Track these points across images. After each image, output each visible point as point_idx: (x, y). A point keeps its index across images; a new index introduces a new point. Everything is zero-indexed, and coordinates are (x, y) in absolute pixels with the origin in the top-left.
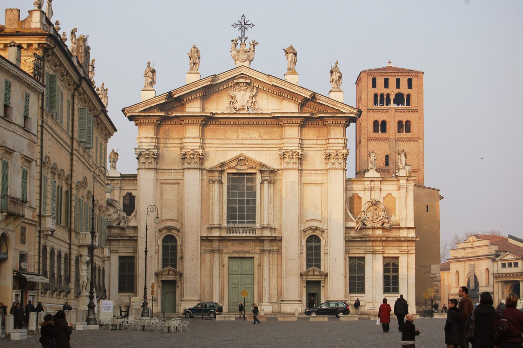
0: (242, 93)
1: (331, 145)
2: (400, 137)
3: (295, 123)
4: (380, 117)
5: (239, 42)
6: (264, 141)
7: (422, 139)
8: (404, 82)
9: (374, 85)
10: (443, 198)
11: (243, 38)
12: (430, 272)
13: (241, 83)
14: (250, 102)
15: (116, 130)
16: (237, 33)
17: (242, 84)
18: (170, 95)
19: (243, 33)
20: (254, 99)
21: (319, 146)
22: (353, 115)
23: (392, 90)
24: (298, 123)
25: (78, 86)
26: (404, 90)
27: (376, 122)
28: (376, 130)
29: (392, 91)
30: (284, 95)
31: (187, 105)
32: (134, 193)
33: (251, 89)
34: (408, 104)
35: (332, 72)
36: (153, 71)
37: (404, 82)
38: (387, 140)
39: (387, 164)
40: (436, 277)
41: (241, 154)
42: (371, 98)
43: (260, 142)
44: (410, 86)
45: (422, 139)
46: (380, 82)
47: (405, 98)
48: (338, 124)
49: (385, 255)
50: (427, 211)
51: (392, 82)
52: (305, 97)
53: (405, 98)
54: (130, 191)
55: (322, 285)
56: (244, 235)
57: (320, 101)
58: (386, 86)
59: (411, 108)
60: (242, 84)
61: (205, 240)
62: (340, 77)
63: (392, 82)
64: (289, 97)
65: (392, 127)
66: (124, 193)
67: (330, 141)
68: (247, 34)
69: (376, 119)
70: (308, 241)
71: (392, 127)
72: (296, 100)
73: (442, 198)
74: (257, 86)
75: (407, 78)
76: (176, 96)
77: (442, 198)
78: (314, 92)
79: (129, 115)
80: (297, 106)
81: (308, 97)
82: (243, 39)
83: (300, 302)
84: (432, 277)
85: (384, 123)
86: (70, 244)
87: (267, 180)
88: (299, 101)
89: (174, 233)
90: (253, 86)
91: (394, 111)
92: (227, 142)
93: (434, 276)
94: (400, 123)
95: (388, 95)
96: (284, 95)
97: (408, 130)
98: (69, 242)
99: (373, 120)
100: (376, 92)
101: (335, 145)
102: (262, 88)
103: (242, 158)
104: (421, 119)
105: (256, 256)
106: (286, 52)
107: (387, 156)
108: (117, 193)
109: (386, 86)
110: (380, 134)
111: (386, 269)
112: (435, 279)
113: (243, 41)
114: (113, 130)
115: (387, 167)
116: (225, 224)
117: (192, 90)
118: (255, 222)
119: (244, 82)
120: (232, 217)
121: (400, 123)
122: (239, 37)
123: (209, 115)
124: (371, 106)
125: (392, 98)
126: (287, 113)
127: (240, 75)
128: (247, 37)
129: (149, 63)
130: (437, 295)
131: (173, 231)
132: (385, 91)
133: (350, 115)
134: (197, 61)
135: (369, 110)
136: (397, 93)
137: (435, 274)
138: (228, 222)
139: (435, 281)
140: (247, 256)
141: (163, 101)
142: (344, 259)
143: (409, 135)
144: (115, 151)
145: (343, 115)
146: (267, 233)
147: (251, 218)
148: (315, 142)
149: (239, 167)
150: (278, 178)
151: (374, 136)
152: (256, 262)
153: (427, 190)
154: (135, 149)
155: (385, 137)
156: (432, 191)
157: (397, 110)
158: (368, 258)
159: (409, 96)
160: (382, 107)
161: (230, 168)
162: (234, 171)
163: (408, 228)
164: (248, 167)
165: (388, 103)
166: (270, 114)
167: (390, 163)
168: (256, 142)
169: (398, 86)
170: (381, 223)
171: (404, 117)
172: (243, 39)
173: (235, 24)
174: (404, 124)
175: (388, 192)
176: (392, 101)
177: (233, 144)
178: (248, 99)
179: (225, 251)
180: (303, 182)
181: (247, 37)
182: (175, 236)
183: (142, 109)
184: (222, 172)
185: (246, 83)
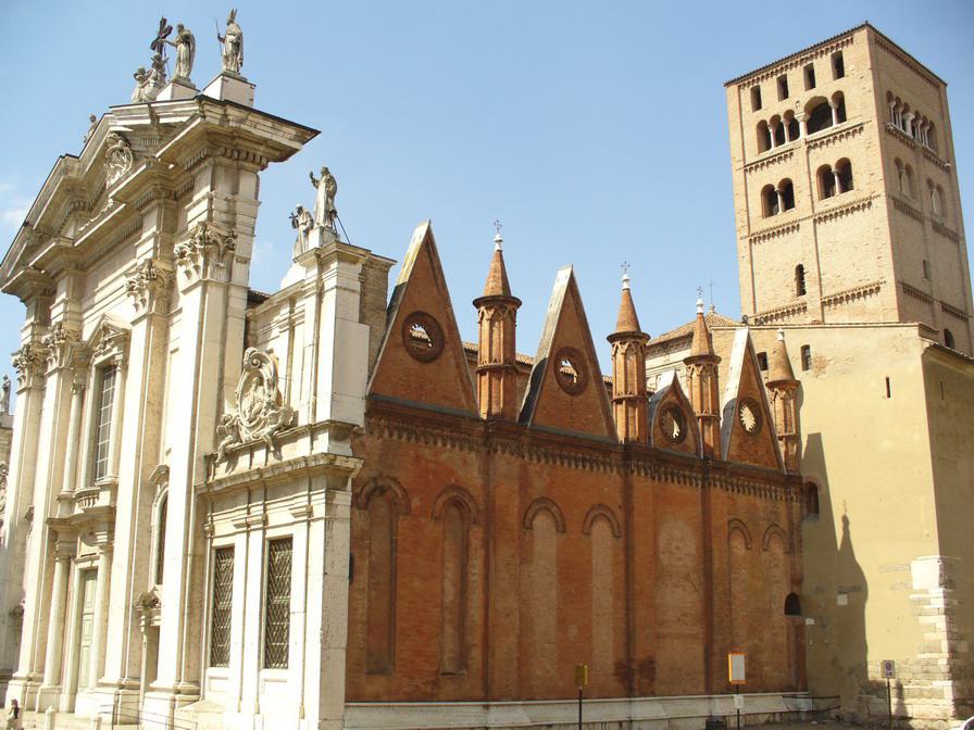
2: (827, 208)
4: (773, 176)
8: (823, 65)
9: (758, 105)
12: (907, 586)
22: (199, 120)
24: (151, 200)
26: (826, 87)
27: (769, 193)
28: (770, 210)
34: (842, 118)
37: (823, 65)
39: (802, 292)
41: (104, 316)
42: (752, 135)
44: (839, 71)
46: (769, 88)
47: (830, 101)
49: (271, 534)
50: (889, 396)
51: (796, 77)
57: (162, 121)
58: (784, 92)
59: (845, 125)
61: (55, 528)
62: (237, 45)
63: (796, 77)
75: (830, 54)
81: (148, 122)
84: (919, 602)
85: (787, 186)
93: (923, 596)
94: (825, 175)
95: (789, 114)
97: (847, 185)
100: (761, 118)
107: (800, 270)
109: (784, 92)
110: (782, 217)
112: (926, 607)
115: (803, 298)
119: (114, 150)
121: (825, 175)
124: (753, 155)
125: (800, 115)
130: (937, 659)
137: (927, 593)
140: (96, 563)
142: (186, 555)
146: (104, 499)
149: (108, 347)
155: (790, 220)
157: (811, 146)
159: (839, 98)
160: (782, 148)
163: (313, 431)
165: (794, 135)
167: (807, 287)
169: (811, 81)
171: (829, 156)
179: (78, 557)
180: (169, 351)
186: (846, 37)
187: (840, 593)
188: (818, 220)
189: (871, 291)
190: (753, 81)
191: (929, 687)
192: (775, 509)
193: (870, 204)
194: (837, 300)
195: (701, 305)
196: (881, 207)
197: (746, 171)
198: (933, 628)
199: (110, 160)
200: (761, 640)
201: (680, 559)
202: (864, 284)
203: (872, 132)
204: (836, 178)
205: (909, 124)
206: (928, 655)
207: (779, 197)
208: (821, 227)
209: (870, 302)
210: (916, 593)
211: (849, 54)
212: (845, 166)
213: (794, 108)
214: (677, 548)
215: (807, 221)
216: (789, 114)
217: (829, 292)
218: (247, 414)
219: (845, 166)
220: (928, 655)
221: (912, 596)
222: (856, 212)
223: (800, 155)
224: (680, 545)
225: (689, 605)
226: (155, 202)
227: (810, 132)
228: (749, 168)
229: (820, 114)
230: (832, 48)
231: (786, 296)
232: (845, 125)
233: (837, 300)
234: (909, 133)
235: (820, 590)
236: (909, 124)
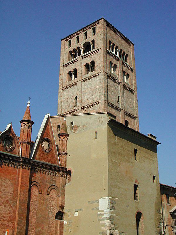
2: (86, 77)
12: (97, 209)
27: (70, 73)
34: (93, 48)
39: (76, 105)
40: (103, 215)
47: (91, 43)
59: (94, 50)
65: (81, 70)
75: (92, 28)
84: (99, 215)
93: (102, 213)
95: (78, 48)
107: (76, 98)
112: (102, 217)
121: (87, 66)
137: (103, 211)
139: (102, 220)
143: (93, 73)
159: (93, 41)
165: (80, 54)
171: (88, 60)
174: (90, 64)
176: (82, 52)
186: (96, 22)
188: (83, 81)
189: (97, 104)
192: (55, 179)
193: (99, 75)
194: (86, 107)
195: (29, 104)
196: (102, 75)
197: (64, 67)
198: (104, 225)
200: (43, 228)
201: (4, 194)
202: (95, 102)
203: (101, 52)
204: (90, 67)
205: (118, 53)
207: (73, 74)
209: (96, 108)
210: (100, 211)
211: (97, 28)
213: (80, 46)
214: (4, 190)
215: (80, 82)
216: (78, 48)
217: (85, 105)
221: (98, 213)
222: (94, 78)
223: (80, 61)
224: (5, 189)
225: (7, 213)
227: (84, 53)
229: (87, 47)
230: (93, 26)
231: (71, 108)
232: (94, 50)
233: (86, 107)
234: (118, 55)
235: (69, 210)
236: (118, 53)
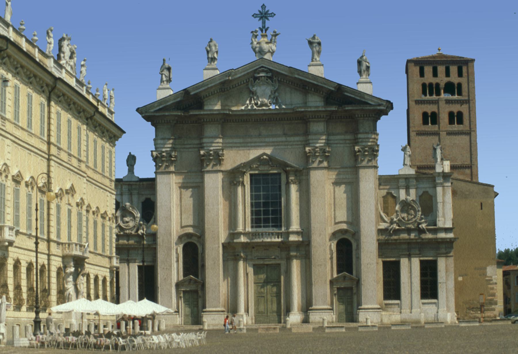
0: (263, 88)
1: (360, 140)
3: (321, 118)
4: (430, 109)
5: (259, 33)
6: (288, 138)
7: (474, 131)
8: (454, 70)
9: (422, 74)
10: (498, 194)
11: (264, 29)
12: (485, 274)
13: (261, 76)
14: (272, 96)
15: (124, 132)
16: (258, 24)
17: (263, 78)
18: (186, 91)
19: (264, 23)
20: (277, 94)
21: (348, 142)
23: (441, 79)
24: (323, 118)
25: (54, 88)
26: (454, 78)
27: (425, 115)
28: (425, 122)
29: (442, 79)
30: (307, 88)
31: (205, 103)
32: (152, 199)
33: (273, 82)
34: (460, 94)
35: (359, 63)
36: (169, 69)
37: (454, 70)
38: (436, 134)
40: (492, 280)
43: (284, 139)
45: (474, 131)
46: (428, 70)
47: (456, 85)
48: (366, 117)
51: (441, 69)
52: (330, 90)
53: (456, 85)
54: (149, 197)
55: (355, 291)
56: (269, 240)
57: (346, 94)
58: (435, 74)
60: (263, 78)
63: (441, 69)
64: (313, 90)
65: (444, 118)
66: (143, 198)
67: (360, 136)
68: (268, 24)
69: (425, 110)
70: (338, 245)
71: (444, 118)
72: (321, 93)
73: (496, 194)
74: (279, 79)
76: (192, 93)
77: (496, 194)
78: (339, 84)
79: (143, 115)
80: (323, 100)
81: (333, 89)
82: (264, 30)
83: (330, 311)
84: (487, 280)
86: (49, 255)
87: (292, 180)
88: (324, 94)
89: (194, 240)
90: (275, 80)
91: (444, 102)
92: (249, 140)
93: (490, 278)
95: (438, 85)
96: (307, 88)
97: (460, 121)
98: (47, 252)
99: (421, 112)
101: (364, 140)
102: (285, 81)
103: (265, 157)
104: (472, 111)
105: (283, 263)
106: (311, 43)
108: (135, 198)
109: (435, 74)
110: (430, 127)
111: (423, 274)
113: (264, 32)
114: (120, 132)
116: (249, 229)
117: (210, 86)
118: (281, 226)
120: (256, 222)
121: (451, 115)
122: (260, 28)
123: (228, 112)
126: (310, 107)
127: (260, 68)
128: (268, 28)
129: (164, 60)
130: (493, 299)
131: (194, 238)
132: (434, 81)
133: (378, 108)
134: (215, 55)
135: (418, 102)
136: (446, 81)
137: (491, 277)
138: (252, 227)
141: (179, 99)
143: (461, 127)
144: (132, 154)
145: (372, 108)
146: (293, 238)
147: (277, 222)
148: (342, 137)
150: (304, 178)
151: (423, 129)
152: (283, 268)
153: (482, 186)
154: (152, 151)
156: (486, 187)
157: (448, 102)
158: (404, 262)
159: (460, 85)
161: (251, 169)
162: (257, 172)
164: (272, 167)
166: (293, 109)
168: (279, 139)
169: (448, 74)
170: (416, 225)
171: (456, 108)
172: (264, 30)
173: (255, 14)
174: (456, 114)
175: (424, 190)
177: (255, 142)
178: (270, 93)
181: (268, 28)
182: (195, 242)
183: (158, 108)
184: (244, 173)
185: (267, 77)
187: (460, 276)
188: (449, 133)
190: (422, 63)
191: (491, 308)
198: (493, 289)
199: (256, 79)
206: (491, 298)
208: (448, 137)
209: (468, 171)
212: (460, 114)
216: (438, 85)
218: (406, 219)
219: (460, 114)
220: (491, 298)
226: (324, 119)
228: (418, 102)
